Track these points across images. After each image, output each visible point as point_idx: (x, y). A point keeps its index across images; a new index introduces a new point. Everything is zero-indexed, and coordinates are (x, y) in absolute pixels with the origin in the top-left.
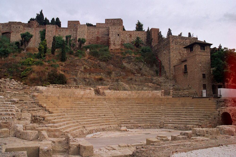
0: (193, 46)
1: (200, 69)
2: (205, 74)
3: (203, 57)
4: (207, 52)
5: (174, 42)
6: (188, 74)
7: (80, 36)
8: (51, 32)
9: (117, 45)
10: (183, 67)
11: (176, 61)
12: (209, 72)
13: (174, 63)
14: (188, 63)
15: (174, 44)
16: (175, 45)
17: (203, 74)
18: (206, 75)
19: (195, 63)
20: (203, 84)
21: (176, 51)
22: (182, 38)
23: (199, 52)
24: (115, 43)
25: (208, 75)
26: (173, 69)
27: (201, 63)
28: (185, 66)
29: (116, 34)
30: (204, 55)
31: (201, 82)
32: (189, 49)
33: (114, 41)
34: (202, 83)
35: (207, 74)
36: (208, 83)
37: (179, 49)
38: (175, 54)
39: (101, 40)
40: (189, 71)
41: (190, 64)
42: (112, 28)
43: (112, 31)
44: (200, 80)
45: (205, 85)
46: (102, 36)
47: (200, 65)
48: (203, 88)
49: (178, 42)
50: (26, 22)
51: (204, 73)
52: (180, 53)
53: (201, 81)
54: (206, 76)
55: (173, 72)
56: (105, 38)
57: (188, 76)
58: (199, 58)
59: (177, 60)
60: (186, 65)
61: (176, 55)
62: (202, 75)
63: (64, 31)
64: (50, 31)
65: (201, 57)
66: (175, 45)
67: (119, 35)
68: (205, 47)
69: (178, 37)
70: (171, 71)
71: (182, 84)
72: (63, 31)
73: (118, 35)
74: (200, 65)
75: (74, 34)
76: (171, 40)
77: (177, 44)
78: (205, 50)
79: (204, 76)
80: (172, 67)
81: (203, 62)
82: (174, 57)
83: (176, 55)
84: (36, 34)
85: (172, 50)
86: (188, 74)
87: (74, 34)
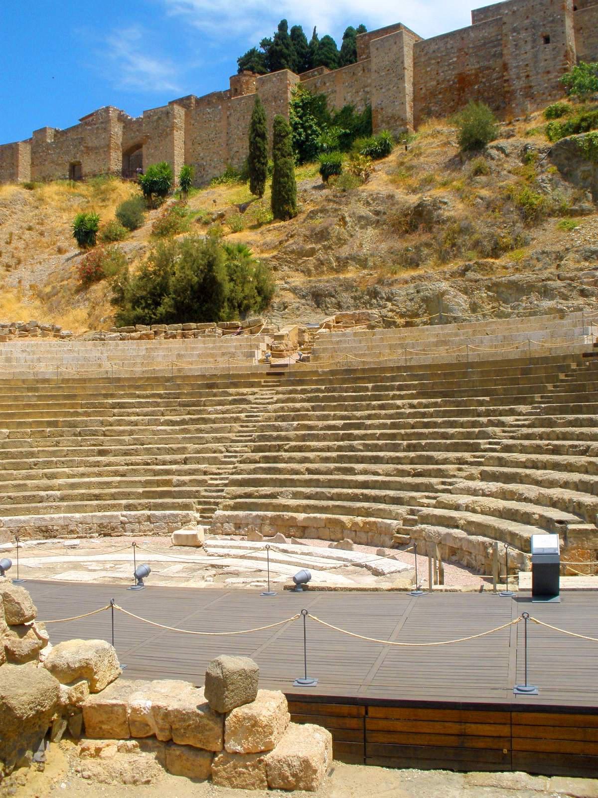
7: (383, 90)
8: (275, 102)
24: (531, 87)
29: (534, 41)
33: (528, 76)
39: (476, 87)
42: (514, 12)
43: (514, 30)
46: (482, 64)
50: (225, 86)
56: (494, 70)
63: (328, 84)
67: (551, 39)
72: (325, 83)
73: (547, 40)
75: (366, 89)
84: (229, 124)
87: (366, 89)
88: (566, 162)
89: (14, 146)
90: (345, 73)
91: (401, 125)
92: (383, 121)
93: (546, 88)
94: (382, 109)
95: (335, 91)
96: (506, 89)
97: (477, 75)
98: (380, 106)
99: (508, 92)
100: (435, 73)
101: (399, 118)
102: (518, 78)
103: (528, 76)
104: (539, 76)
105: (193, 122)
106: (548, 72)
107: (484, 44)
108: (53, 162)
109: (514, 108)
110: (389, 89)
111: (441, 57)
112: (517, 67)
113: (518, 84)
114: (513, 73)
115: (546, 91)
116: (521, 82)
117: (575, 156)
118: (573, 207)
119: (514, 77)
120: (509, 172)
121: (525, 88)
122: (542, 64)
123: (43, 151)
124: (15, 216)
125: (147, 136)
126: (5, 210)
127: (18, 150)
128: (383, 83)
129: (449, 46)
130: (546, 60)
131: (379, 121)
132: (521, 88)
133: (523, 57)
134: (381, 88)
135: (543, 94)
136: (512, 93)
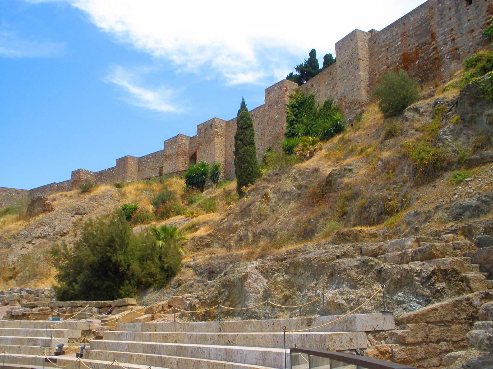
7: (345, 81)
8: (277, 105)
9: (469, 52)
24: (456, 49)
33: (453, 39)
39: (417, 63)
46: (420, 41)
63: (314, 86)
64: (273, 104)
72: (312, 86)
88: (469, 109)
89: (125, 158)
90: (325, 74)
91: (358, 108)
92: (346, 107)
93: (471, 46)
94: (345, 97)
95: (320, 91)
96: (435, 56)
97: (417, 53)
98: (343, 95)
99: (437, 58)
100: (385, 58)
101: (357, 102)
102: (445, 44)
103: (453, 39)
104: (464, 37)
105: (230, 130)
106: (473, 31)
107: (421, 25)
108: (150, 168)
109: (443, 72)
110: (349, 79)
111: (389, 44)
112: (442, 34)
113: (444, 49)
114: (440, 39)
115: (472, 49)
116: (448, 47)
117: (478, 100)
118: (473, 157)
119: (441, 43)
120: (417, 130)
121: (452, 51)
122: (466, 25)
123: (145, 161)
124: (101, 207)
125: (199, 144)
126: (94, 203)
127: (127, 161)
128: (345, 75)
129: (394, 33)
130: (469, 20)
131: (343, 108)
132: (448, 52)
133: (448, 23)
134: (344, 80)
135: (469, 52)
136: (442, 57)
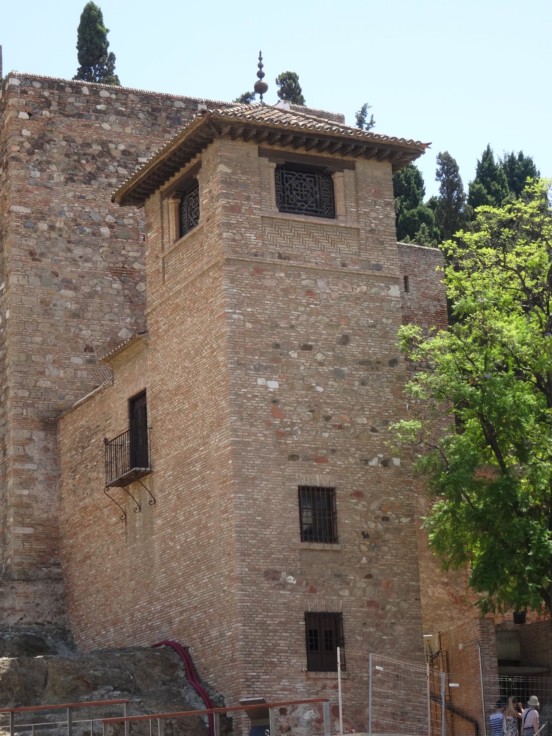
0: (199, 166)
1: (262, 434)
2: (328, 494)
3: (310, 293)
4: (358, 229)
5: (56, 150)
6: (153, 502)
10: (120, 421)
11: (78, 360)
12: (385, 463)
13: (44, 383)
14: (155, 368)
15: (59, 178)
16: (70, 179)
17: (308, 494)
18: (339, 504)
19: (217, 365)
20: (309, 616)
21: (78, 251)
22: (153, 113)
23: (253, 227)
25: (374, 506)
26: (34, 451)
27: (275, 359)
28: (138, 404)
30: (314, 273)
31: (284, 585)
32: (171, 204)
34: (293, 600)
35: (358, 495)
36: (371, 603)
37: (111, 227)
38: (67, 284)
40: (161, 460)
41: (171, 385)
44: (263, 565)
45: (335, 619)
47: (273, 385)
48: (300, 662)
49: (106, 152)
51: (320, 479)
52: (131, 272)
53: (272, 575)
54: (349, 517)
55: (39, 489)
57: (159, 522)
58: (254, 301)
59: (89, 349)
60: (142, 395)
61: (71, 299)
62: (293, 504)
65: (286, 291)
66: (70, 179)
68: (341, 180)
69: (108, 101)
70: (11, 481)
71: (114, 624)
74: (273, 385)
76: (23, 124)
77: (90, 178)
78: (332, 215)
79: (318, 512)
80: (26, 434)
81: (307, 348)
82: (47, 313)
83: (71, 299)
85: (32, 243)
86: (159, 496)
